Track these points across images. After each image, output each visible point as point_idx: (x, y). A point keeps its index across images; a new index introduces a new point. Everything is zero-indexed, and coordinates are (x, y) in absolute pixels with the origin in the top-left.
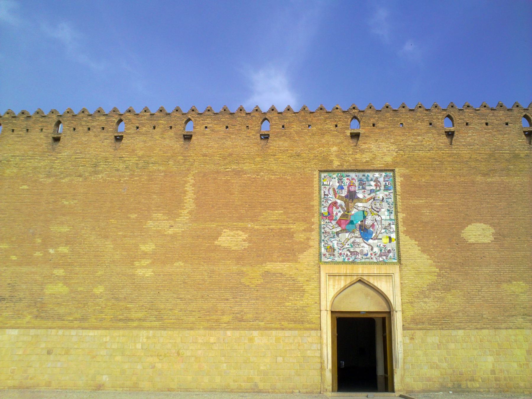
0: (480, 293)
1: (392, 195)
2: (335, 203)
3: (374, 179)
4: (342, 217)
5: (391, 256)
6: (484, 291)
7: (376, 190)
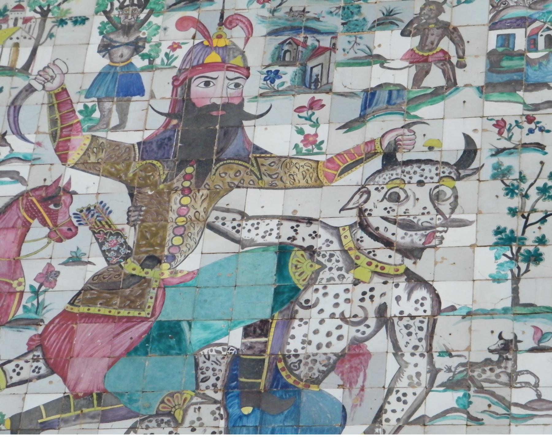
4: (92, 302)
7: (417, 92)
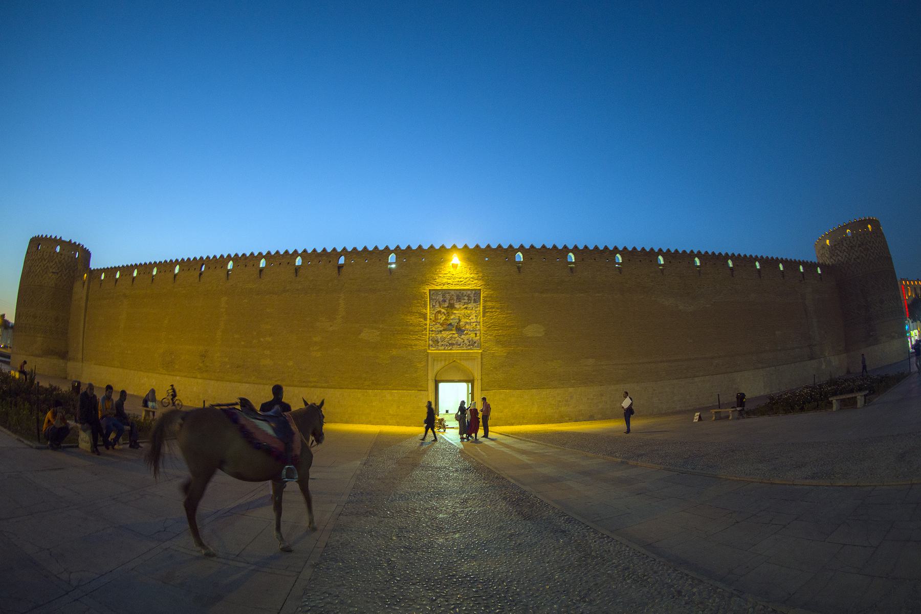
3: (467, 295)
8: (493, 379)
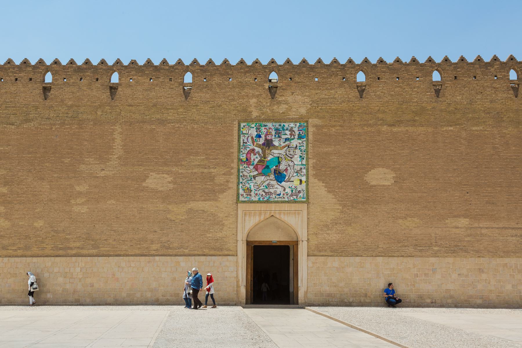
0: (377, 227)
1: (305, 143)
2: (253, 150)
3: (289, 128)
4: (259, 163)
5: (300, 196)
6: (381, 226)
8: (324, 241)
